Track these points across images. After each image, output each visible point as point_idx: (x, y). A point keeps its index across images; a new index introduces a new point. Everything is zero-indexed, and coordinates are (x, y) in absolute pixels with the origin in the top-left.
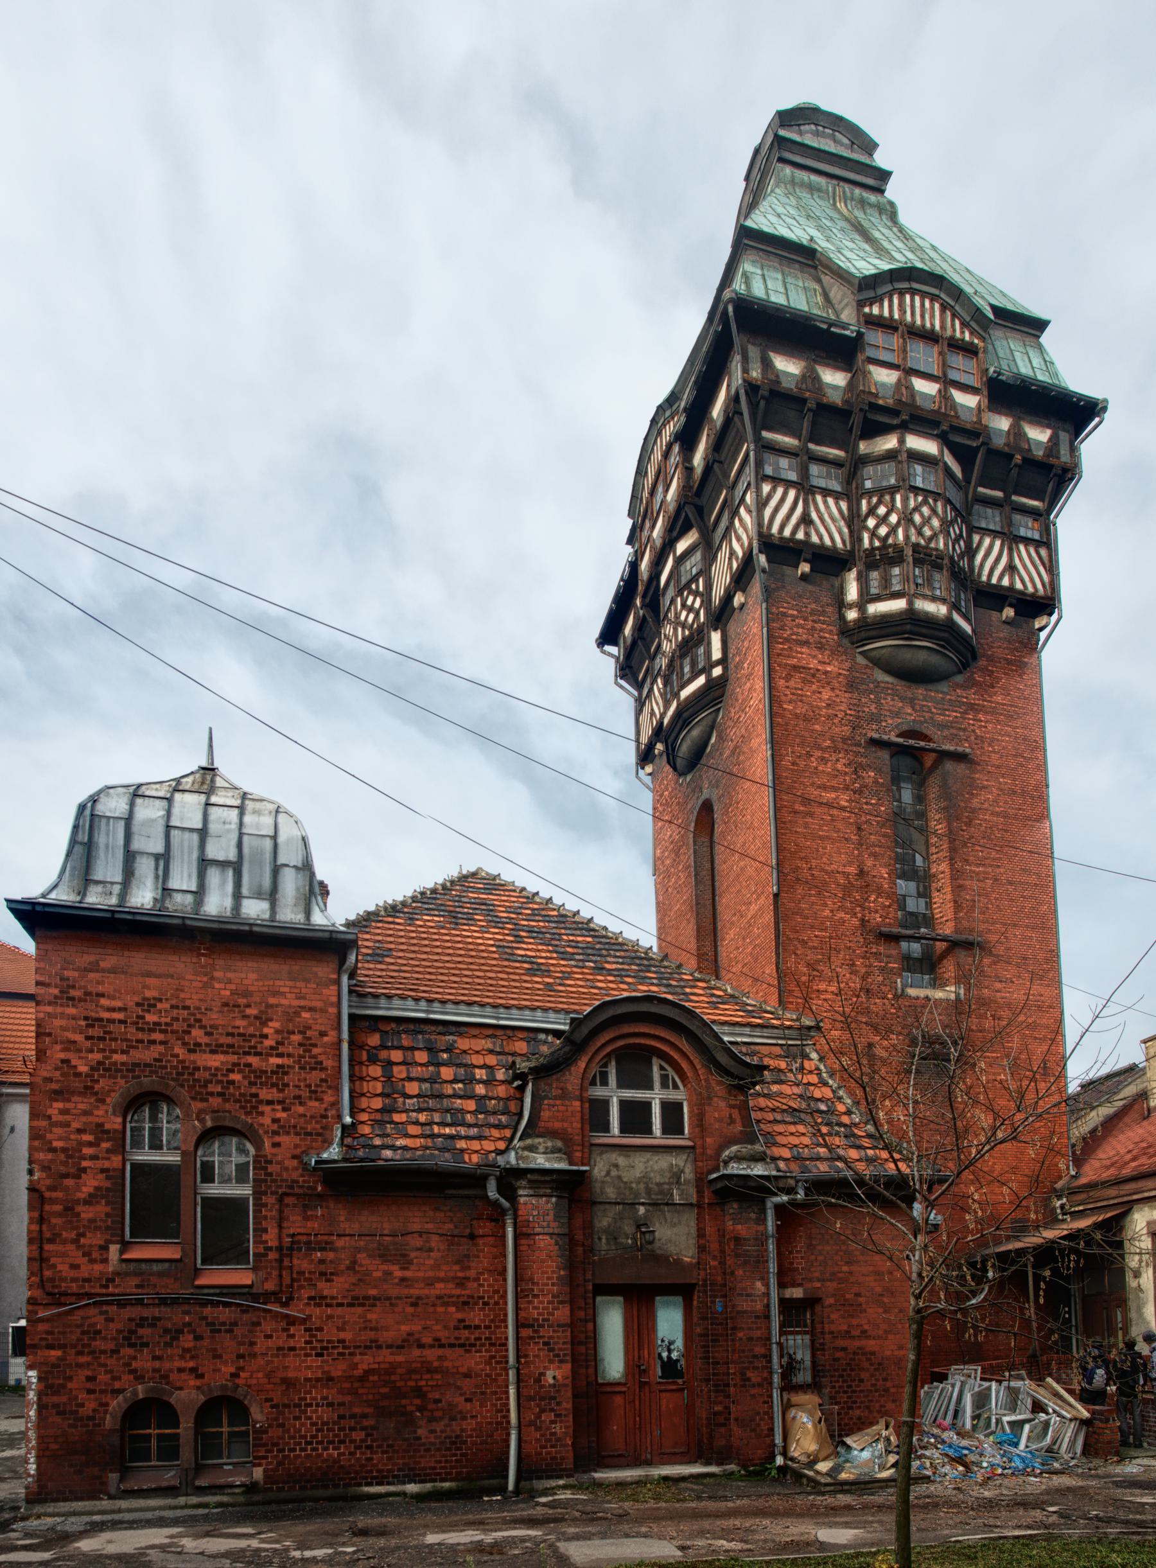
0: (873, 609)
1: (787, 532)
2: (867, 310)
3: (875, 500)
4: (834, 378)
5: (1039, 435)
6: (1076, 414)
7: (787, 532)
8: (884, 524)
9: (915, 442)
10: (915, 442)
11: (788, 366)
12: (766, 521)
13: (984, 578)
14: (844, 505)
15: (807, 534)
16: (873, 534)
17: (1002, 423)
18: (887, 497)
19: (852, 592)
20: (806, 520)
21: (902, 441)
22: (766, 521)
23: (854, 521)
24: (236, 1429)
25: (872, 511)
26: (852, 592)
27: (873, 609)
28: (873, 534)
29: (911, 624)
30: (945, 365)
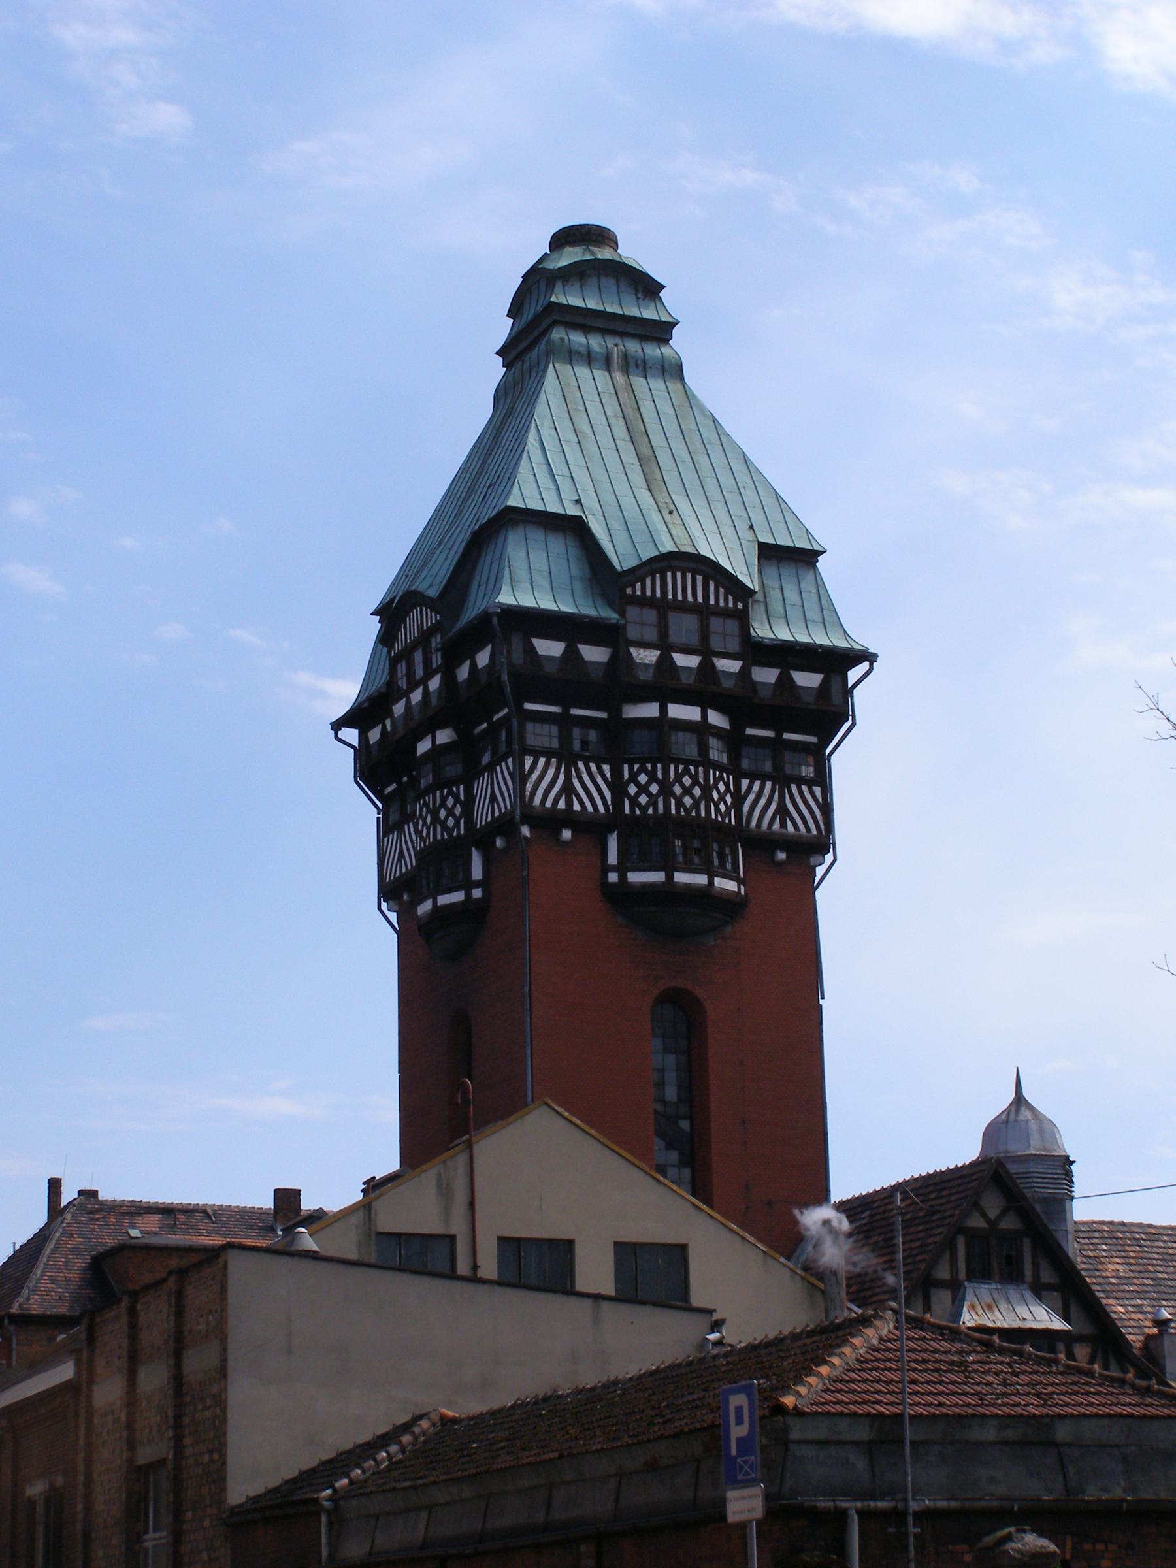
1: (548, 804)
2: (629, 591)
3: (636, 767)
4: (594, 654)
5: (807, 680)
6: (838, 662)
7: (548, 804)
8: (643, 793)
9: (677, 711)
10: (677, 711)
11: (550, 648)
12: (528, 794)
13: (753, 824)
14: (606, 768)
15: (569, 803)
16: (634, 802)
17: (766, 675)
18: (649, 766)
19: (613, 858)
20: (568, 789)
21: (663, 710)
22: (528, 794)
23: (618, 788)
25: (633, 778)
26: (613, 858)
27: (635, 877)
28: (634, 802)
29: (668, 894)
30: (705, 634)
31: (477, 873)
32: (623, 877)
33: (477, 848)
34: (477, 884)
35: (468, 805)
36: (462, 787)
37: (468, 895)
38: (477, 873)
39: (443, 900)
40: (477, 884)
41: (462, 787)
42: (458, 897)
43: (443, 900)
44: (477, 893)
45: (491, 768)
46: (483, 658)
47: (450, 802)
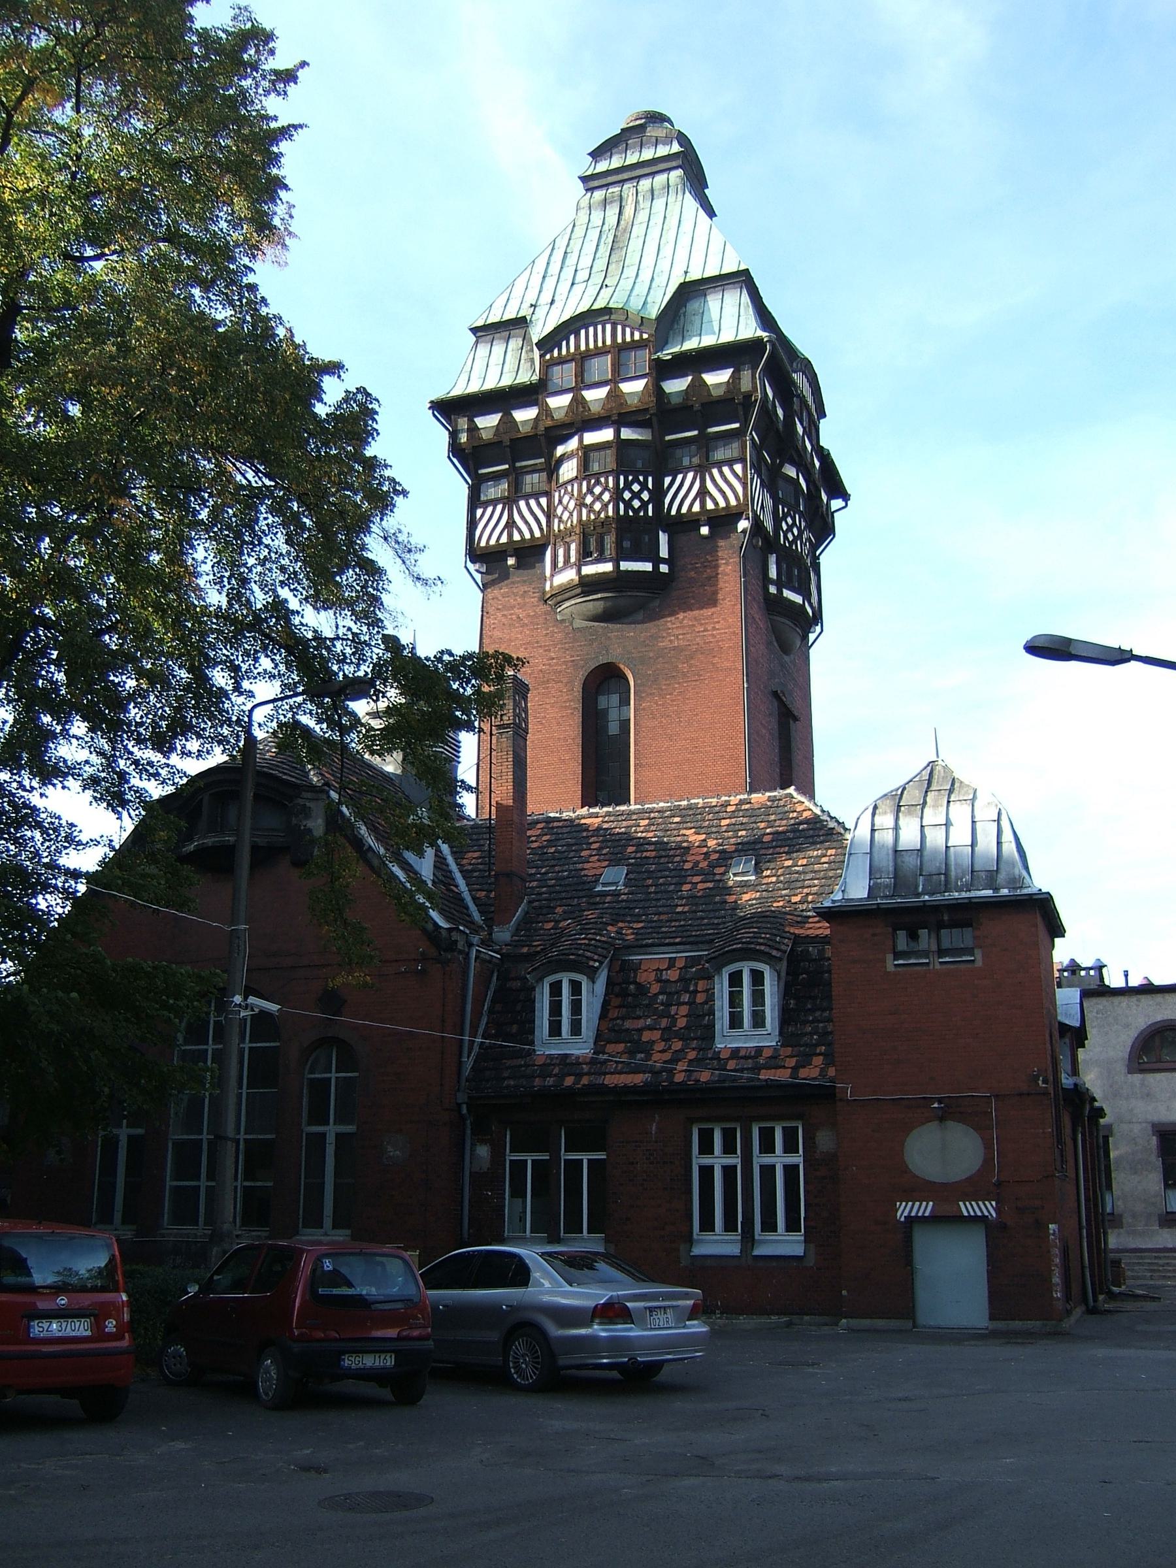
0: (787, 593)
19: (773, 573)
24: (330, 1150)
26: (773, 573)
27: (787, 593)
31: (664, 553)
32: (780, 591)
33: (664, 532)
34: (664, 561)
35: (658, 494)
36: (650, 479)
37: (656, 567)
38: (664, 553)
39: (625, 566)
40: (664, 561)
41: (650, 479)
42: (648, 567)
43: (625, 566)
44: (664, 568)
45: (701, 470)
46: (717, 379)
47: (636, 487)
